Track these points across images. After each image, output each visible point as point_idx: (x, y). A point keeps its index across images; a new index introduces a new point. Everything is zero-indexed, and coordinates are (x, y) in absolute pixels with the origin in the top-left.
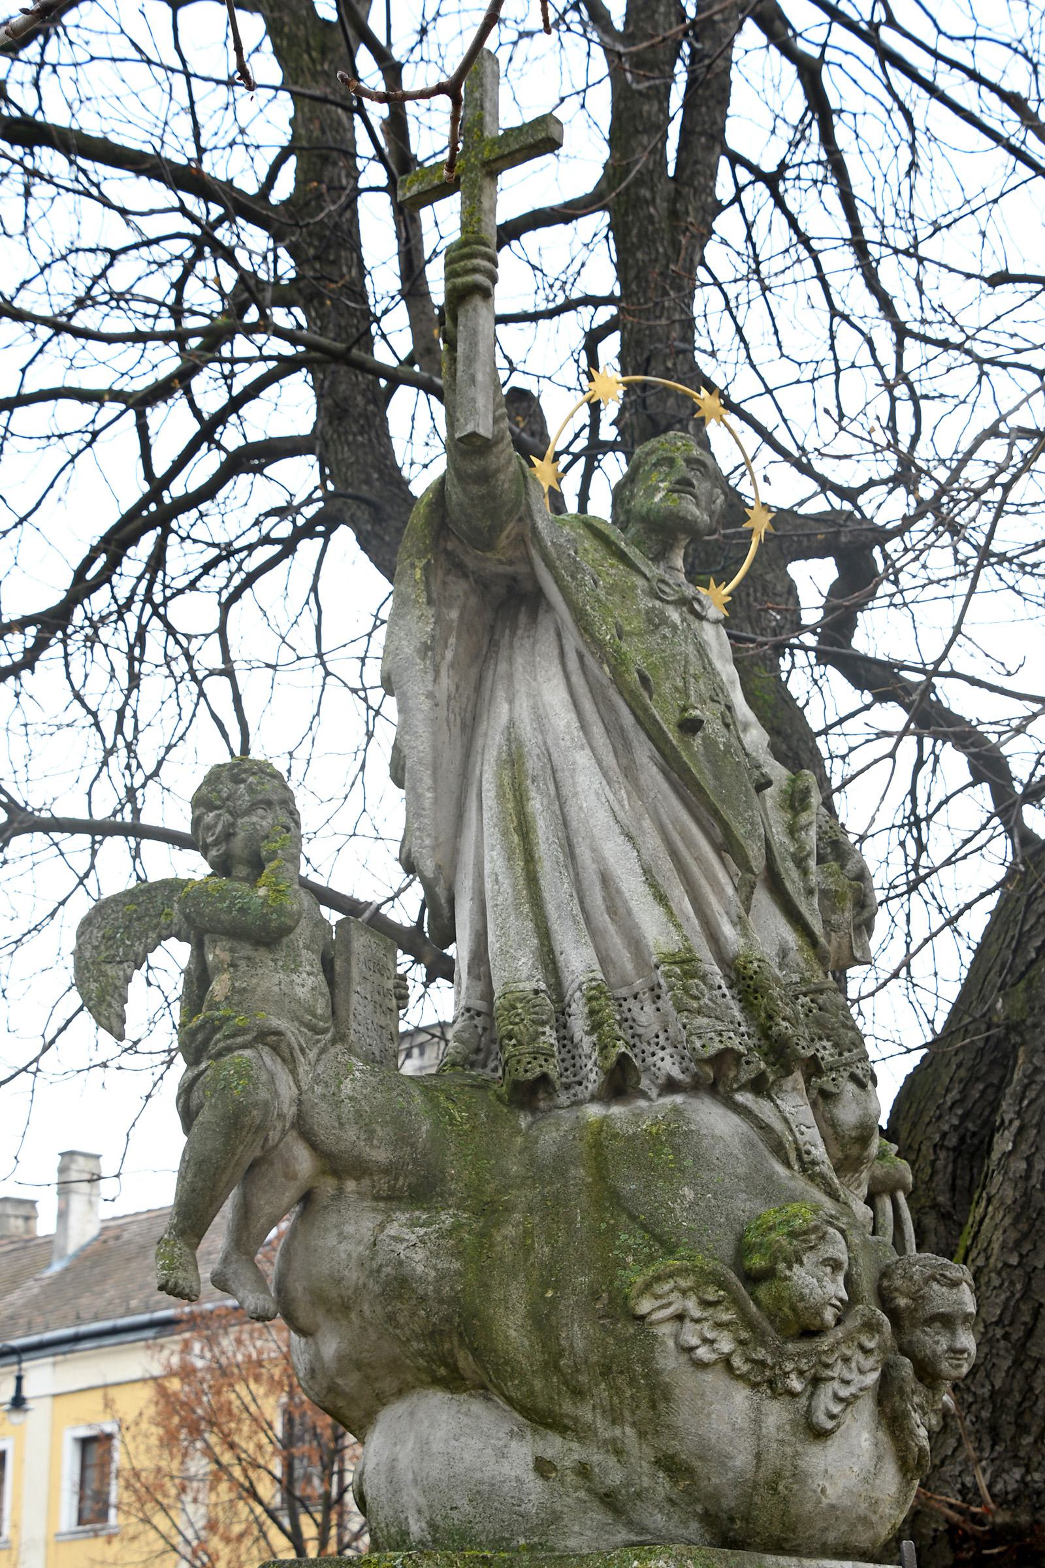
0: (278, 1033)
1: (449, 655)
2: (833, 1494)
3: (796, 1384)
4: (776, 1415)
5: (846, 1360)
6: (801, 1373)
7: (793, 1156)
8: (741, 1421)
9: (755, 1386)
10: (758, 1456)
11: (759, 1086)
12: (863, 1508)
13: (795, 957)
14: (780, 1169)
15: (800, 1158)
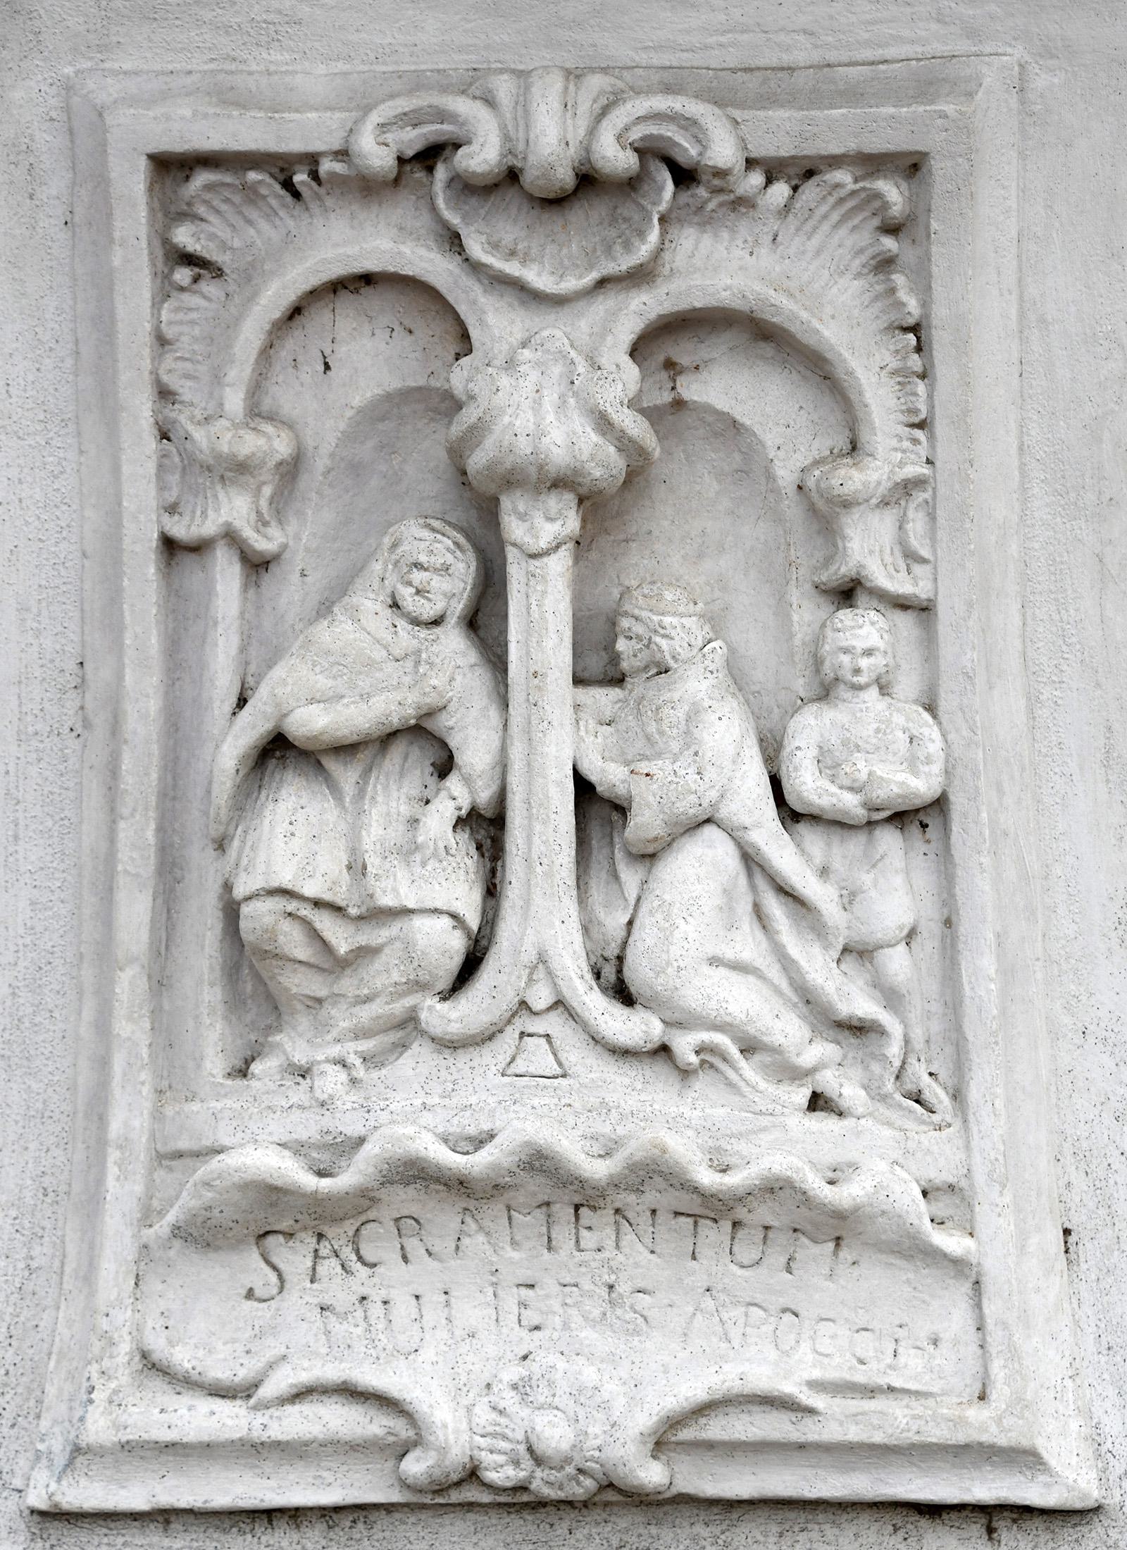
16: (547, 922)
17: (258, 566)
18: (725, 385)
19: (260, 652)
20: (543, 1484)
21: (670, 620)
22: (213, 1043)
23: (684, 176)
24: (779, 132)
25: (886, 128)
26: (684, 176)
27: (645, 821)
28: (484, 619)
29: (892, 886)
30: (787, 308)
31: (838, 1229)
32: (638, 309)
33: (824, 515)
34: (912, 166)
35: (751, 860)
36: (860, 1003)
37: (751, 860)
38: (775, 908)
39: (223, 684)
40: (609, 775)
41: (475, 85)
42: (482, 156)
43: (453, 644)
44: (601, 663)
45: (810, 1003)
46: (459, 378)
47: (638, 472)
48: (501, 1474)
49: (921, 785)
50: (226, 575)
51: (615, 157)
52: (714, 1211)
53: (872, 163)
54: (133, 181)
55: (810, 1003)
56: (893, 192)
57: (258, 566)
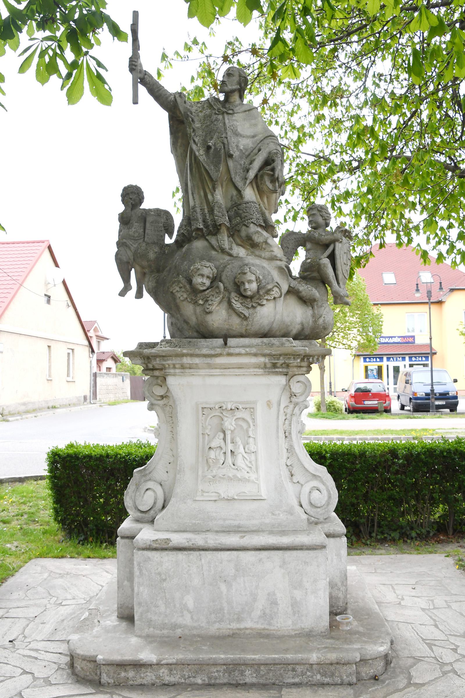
0: (125, 243)
1: (179, 144)
2: (216, 325)
3: (201, 302)
4: (199, 310)
5: (213, 295)
6: (202, 300)
7: (218, 249)
8: (192, 312)
9: (194, 303)
10: (197, 318)
11: (211, 233)
12: (227, 327)
13: (235, 198)
14: (214, 253)
15: (220, 249)
16: (229, 460)
17: (208, 435)
18: (241, 423)
19: (210, 442)
20: (229, 498)
21: (238, 439)
22: (206, 469)
23: (238, 409)
24: (244, 406)
25: (252, 406)
26: (238, 409)
27: (236, 453)
28: (224, 439)
29: (253, 457)
30: (245, 418)
31: (248, 481)
32: (235, 418)
33: (247, 431)
34: (253, 408)
35: (243, 456)
36: (251, 466)
37: (243, 456)
38: (245, 459)
39: (206, 444)
40: (233, 450)
41: (224, 403)
42: (224, 408)
43: (222, 441)
44: (232, 442)
45: (247, 465)
46: (222, 422)
47: (235, 429)
48: (226, 498)
49: (254, 451)
50: (207, 436)
51: (233, 408)
52: (239, 480)
53: (250, 408)
54: (200, 409)
55: (247, 465)
56: (252, 410)
57: (208, 435)
